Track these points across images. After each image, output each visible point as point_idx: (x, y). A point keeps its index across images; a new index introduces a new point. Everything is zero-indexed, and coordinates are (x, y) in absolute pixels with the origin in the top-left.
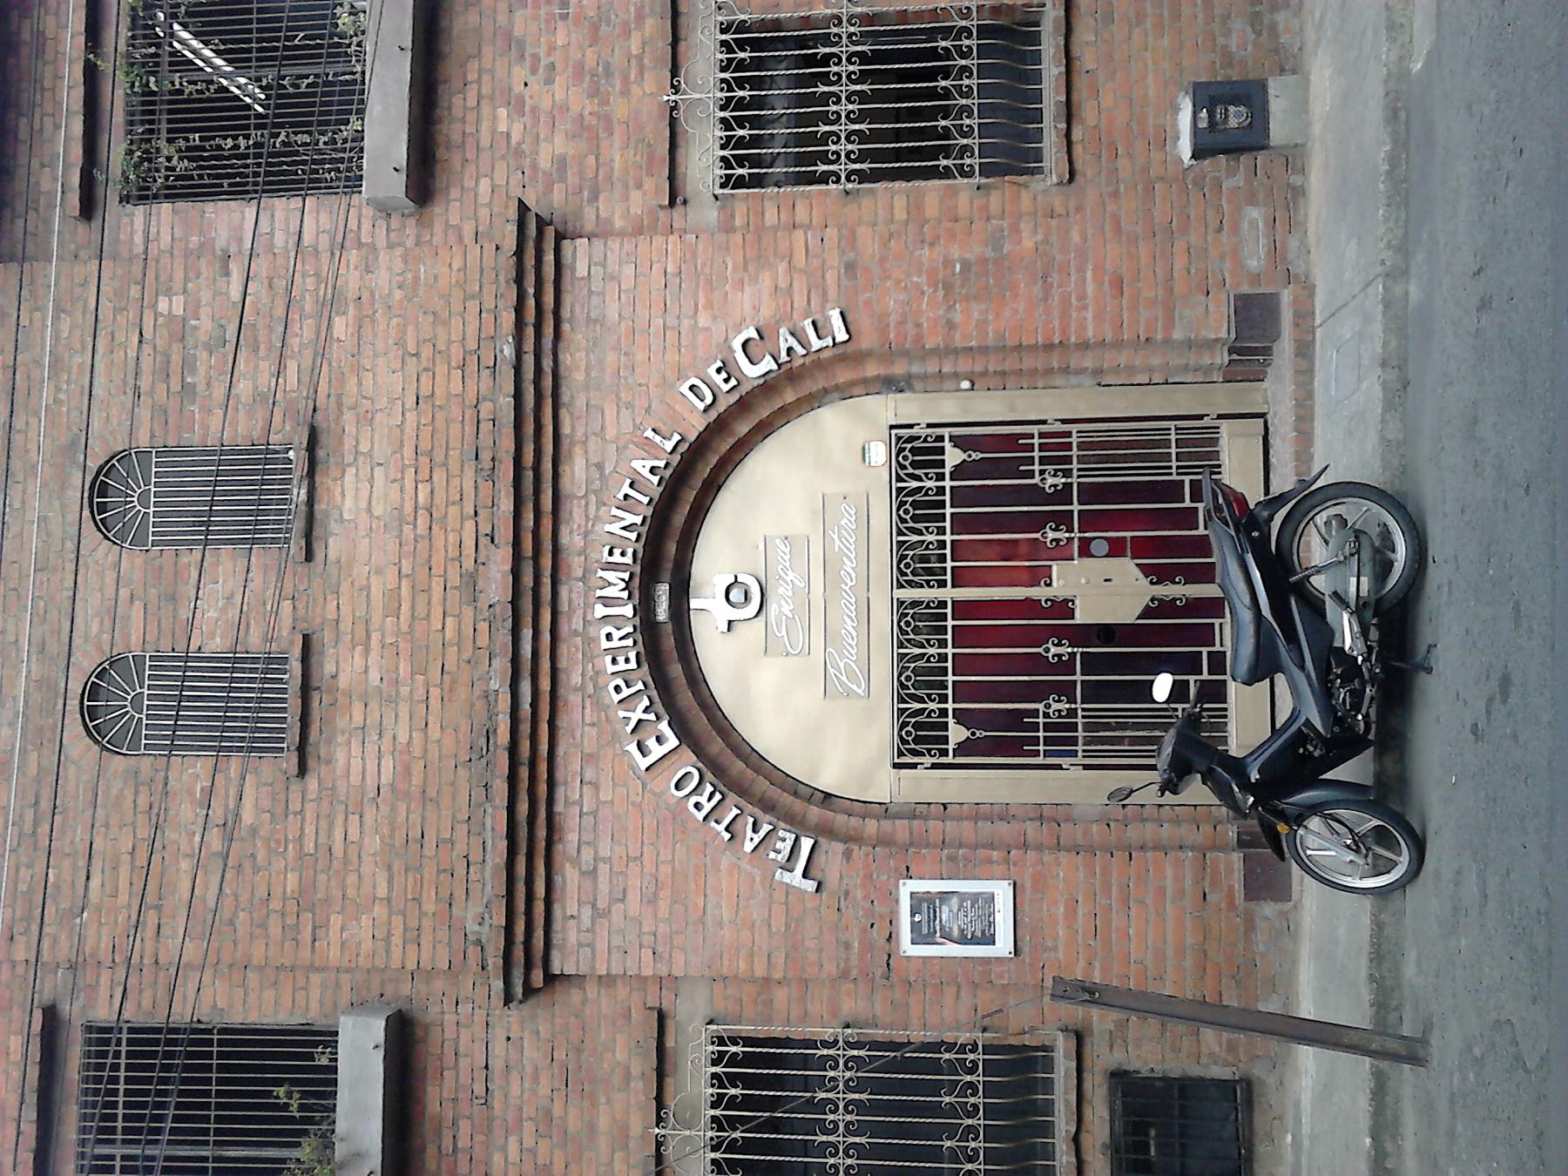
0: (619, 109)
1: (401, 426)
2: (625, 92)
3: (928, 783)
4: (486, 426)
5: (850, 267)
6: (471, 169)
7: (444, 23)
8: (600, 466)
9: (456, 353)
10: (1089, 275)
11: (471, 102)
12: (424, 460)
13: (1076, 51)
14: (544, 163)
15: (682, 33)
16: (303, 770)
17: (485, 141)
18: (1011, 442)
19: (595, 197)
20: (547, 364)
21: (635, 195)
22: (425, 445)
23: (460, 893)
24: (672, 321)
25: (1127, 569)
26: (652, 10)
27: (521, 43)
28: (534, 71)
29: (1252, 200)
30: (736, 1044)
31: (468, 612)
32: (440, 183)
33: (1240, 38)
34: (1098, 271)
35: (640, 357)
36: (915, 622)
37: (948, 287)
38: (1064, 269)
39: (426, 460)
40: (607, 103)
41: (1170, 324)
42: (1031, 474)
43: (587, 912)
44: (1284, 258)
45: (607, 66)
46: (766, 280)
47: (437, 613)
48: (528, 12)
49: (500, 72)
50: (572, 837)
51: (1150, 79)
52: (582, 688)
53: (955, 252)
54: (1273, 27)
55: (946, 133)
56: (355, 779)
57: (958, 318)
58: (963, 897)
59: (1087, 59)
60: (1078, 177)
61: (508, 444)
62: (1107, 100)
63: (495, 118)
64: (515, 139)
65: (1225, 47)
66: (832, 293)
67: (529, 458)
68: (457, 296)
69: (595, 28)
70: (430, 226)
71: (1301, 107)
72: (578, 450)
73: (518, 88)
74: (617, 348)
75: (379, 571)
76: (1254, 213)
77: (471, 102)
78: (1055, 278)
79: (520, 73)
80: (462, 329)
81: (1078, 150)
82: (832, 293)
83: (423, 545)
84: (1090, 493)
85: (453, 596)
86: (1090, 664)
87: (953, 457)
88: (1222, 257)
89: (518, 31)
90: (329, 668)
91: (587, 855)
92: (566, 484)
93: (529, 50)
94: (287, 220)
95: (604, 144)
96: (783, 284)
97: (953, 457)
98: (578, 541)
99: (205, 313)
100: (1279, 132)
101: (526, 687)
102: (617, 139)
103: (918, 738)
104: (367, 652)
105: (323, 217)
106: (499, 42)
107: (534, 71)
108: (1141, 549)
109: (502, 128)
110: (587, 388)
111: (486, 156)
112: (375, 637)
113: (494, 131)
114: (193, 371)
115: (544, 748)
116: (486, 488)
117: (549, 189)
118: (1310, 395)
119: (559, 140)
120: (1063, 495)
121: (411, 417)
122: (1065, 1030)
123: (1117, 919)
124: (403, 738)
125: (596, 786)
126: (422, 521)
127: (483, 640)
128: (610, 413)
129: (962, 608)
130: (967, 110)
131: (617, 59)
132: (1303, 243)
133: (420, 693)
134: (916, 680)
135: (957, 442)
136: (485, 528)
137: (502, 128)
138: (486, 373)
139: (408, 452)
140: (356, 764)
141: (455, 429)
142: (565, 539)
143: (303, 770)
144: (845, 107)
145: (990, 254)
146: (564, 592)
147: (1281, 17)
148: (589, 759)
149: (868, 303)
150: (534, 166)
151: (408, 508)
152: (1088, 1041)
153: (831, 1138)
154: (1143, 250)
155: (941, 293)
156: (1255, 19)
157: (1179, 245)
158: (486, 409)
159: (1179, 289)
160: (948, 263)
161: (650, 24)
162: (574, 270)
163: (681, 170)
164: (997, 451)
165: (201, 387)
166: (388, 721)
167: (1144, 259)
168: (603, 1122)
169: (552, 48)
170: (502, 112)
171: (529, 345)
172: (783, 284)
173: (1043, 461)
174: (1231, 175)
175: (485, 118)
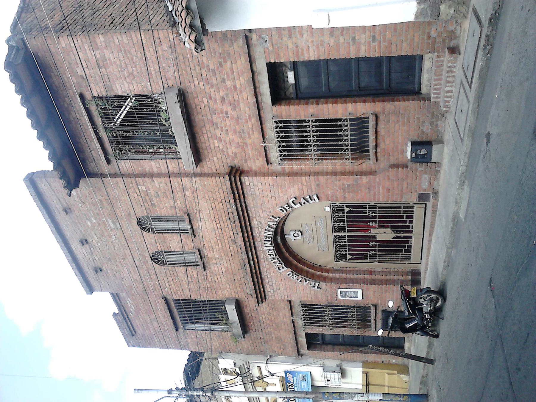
0: (249, 141)
1: (210, 213)
2: (249, 136)
3: (342, 264)
4: (231, 214)
5: (318, 185)
6: (210, 155)
7: (192, 118)
8: (260, 222)
9: (220, 200)
10: (381, 188)
11: (206, 138)
12: (217, 220)
13: (379, 129)
14: (231, 154)
15: (263, 122)
16: (205, 270)
17: (213, 148)
18: (361, 207)
19: (246, 162)
20: (243, 204)
21: (257, 162)
22: (216, 217)
23: (245, 288)
24: (273, 195)
25: (389, 230)
26: (253, 116)
27: (216, 124)
28: (222, 131)
29: (425, 173)
30: (283, 143)
31: (235, 246)
32: (203, 157)
33: (427, 128)
34: (383, 188)
35: (266, 202)
36: (338, 239)
37: (344, 190)
38: (374, 187)
39: (217, 219)
40: (245, 140)
41: (401, 198)
42: (366, 213)
43: (272, 291)
44: (433, 186)
45: (243, 130)
46: (296, 186)
47: (227, 246)
48: (217, 115)
49: (213, 131)
50: (267, 281)
51: (400, 137)
52: (264, 259)
53: (345, 182)
54: (437, 125)
55: (341, 136)
56: (217, 271)
57: (347, 196)
58: (351, 292)
59: (382, 131)
60: (378, 161)
61: (236, 217)
62: (387, 142)
63: (214, 143)
64: (221, 148)
65: (422, 130)
66: (314, 190)
67: (254, 271)
68: (216, 189)
69: (237, 121)
70: (203, 167)
71: (441, 153)
72: (254, 219)
73: (219, 136)
74: (260, 200)
75: (212, 239)
76: (426, 176)
77: (206, 138)
78: (372, 189)
79: (218, 132)
80: (219, 195)
81: (379, 154)
82: (314, 190)
83: (221, 235)
84: (380, 217)
85: (231, 244)
86: (379, 246)
87: (346, 209)
88: (416, 185)
89: (215, 121)
90: (206, 254)
91: (270, 283)
92: (252, 225)
93: (219, 126)
94: (163, 165)
95: (246, 150)
96: (301, 188)
97: (346, 209)
98: (258, 235)
99: (151, 190)
100: (434, 159)
101: (252, 262)
102: (249, 148)
103: (339, 258)
104: (213, 252)
105: (173, 164)
106: (210, 123)
107: (222, 131)
108: (392, 227)
109: (217, 145)
110: (254, 207)
111: (214, 152)
112: (214, 250)
113: (214, 145)
114: (153, 201)
115: (258, 269)
116: (233, 225)
117: (233, 160)
118: (435, 220)
119: (233, 148)
120: (375, 217)
121: (211, 212)
122: (373, 305)
123: (384, 294)
124: (225, 265)
125: (270, 273)
126: (220, 230)
127: (239, 250)
128: (261, 212)
129: (349, 236)
130: (348, 150)
131: (245, 128)
132: (438, 183)
133: (227, 258)
134: (338, 249)
135: (347, 206)
136: (235, 232)
137: (217, 145)
138: (228, 204)
139: (213, 218)
140: (216, 269)
141: (223, 214)
142: (254, 234)
143: (205, 270)
144: (311, 129)
145: (354, 183)
146: (256, 243)
147: (439, 123)
148: (267, 269)
149: (323, 192)
150: (228, 154)
151: (216, 228)
152: (377, 307)
153: (308, 124)
154: (395, 184)
155: (342, 191)
156: (432, 123)
157: (405, 183)
158: (230, 211)
159: (404, 191)
160: (344, 185)
161: (243, 59)
162: (245, 184)
163: (269, 156)
164: (357, 210)
165: (156, 204)
166: (222, 262)
167: (395, 185)
168: (281, 314)
169: (226, 126)
170: (216, 141)
171: (238, 203)
172: (301, 188)
173: (369, 211)
174: (420, 168)
175: (210, 141)
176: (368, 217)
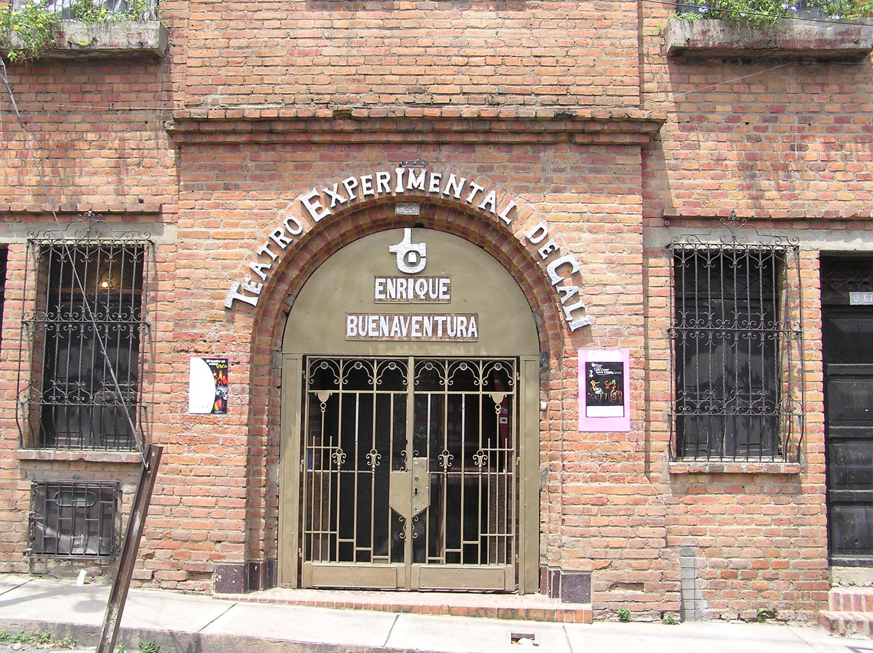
12: (499, 60)
17: (709, 97)
22: (508, 61)
23: (231, 89)
25: (423, 502)
27: (775, 120)
28: (756, 129)
31: (401, 89)
42: (485, 445)
48: (796, 125)
51: (737, 527)
63: (725, 103)
73: (745, 119)
83: (444, 61)
87: (498, 397)
93: (771, 125)
97: (498, 397)
107: (756, 129)
112: (388, 33)
126: (461, 60)
129: (401, 400)
135: (507, 401)
137: (719, 108)
139: (505, 50)
140: (311, 23)
141: (518, 79)
151: (469, 52)
163: (687, 224)
168: (96, 179)
176: (471, 451)
